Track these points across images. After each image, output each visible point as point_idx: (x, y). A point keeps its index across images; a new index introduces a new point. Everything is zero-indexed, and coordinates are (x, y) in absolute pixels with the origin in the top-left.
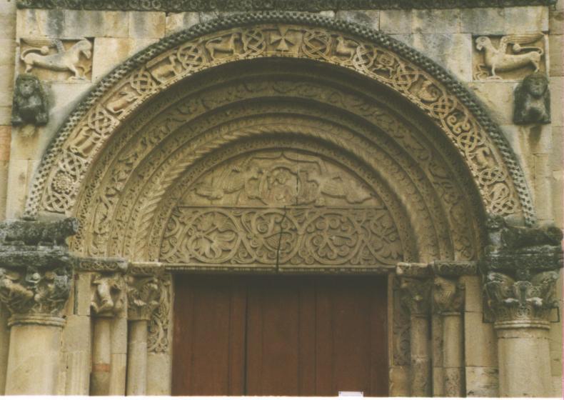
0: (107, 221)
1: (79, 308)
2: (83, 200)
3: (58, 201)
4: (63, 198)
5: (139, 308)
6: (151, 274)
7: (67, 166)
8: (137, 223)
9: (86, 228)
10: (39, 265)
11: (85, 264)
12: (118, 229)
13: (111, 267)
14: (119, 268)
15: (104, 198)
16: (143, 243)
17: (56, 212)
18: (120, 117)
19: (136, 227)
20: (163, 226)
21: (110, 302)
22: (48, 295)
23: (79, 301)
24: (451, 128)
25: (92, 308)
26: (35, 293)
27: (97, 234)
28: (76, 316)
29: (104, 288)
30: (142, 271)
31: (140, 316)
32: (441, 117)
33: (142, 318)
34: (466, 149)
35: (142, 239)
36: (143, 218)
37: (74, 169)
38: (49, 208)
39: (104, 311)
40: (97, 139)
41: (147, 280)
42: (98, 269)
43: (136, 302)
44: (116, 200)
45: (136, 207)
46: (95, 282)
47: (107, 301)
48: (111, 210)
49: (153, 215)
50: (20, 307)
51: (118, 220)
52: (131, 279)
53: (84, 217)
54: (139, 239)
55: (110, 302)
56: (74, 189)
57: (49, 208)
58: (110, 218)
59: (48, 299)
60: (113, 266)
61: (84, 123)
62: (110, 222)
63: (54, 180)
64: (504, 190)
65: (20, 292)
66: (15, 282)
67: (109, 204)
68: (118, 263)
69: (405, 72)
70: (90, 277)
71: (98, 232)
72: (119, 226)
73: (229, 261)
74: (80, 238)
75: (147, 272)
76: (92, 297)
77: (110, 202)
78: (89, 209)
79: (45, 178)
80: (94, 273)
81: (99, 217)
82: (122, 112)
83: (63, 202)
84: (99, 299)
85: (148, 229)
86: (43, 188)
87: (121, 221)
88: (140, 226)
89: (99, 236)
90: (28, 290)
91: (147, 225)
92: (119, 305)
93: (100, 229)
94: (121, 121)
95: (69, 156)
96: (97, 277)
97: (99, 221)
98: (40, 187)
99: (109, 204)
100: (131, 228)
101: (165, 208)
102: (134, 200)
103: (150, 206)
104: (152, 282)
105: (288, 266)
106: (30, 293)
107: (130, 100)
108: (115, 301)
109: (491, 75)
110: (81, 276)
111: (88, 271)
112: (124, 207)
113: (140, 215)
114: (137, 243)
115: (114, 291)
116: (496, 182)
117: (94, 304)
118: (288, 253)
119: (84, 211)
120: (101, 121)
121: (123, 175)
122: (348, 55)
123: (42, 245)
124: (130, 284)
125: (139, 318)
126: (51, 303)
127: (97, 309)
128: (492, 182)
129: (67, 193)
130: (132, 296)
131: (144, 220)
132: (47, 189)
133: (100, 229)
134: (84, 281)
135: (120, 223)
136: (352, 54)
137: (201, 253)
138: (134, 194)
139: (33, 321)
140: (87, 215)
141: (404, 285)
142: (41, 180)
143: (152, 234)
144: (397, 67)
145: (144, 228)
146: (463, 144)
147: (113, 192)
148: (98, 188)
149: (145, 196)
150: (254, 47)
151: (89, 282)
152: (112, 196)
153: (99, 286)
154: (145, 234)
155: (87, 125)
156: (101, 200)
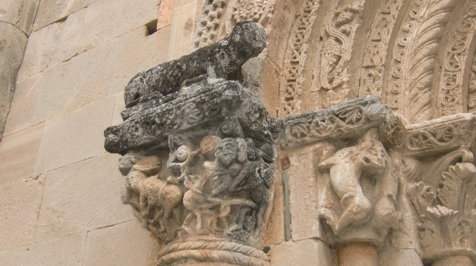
0: (341, 63)
1: (294, 226)
2: (293, 36)
5: (442, 220)
6: (452, 143)
8: (406, 65)
9: (301, 80)
10: (185, 126)
11: (295, 130)
12: (369, 81)
13: (351, 122)
14: (368, 120)
15: (332, 30)
16: (424, 98)
19: (404, 73)
20: (462, 66)
22: (206, 189)
23: (292, 211)
25: (322, 220)
26: (184, 190)
27: (327, 90)
28: (290, 242)
30: (431, 138)
31: (450, 244)
33: (456, 247)
35: (420, 89)
36: (415, 53)
39: (351, 225)
41: (449, 158)
42: (324, 134)
43: (429, 209)
44: (354, 26)
45: (400, 40)
46: (324, 163)
47: (352, 197)
48: (348, 43)
49: (435, 45)
50: (162, 228)
51: (368, 67)
52: (412, 165)
53: (298, 62)
54: (413, 92)
55: (360, 199)
56: (267, 10)
58: (346, 57)
59: (209, 199)
60: (355, 117)
62: (347, 63)
63: (235, 10)
65: (154, 192)
66: (148, 174)
67: (343, 37)
68: (363, 108)
70: (311, 156)
71: (327, 86)
72: (370, 75)
74: (292, 99)
75: (441, 140)
76: (323, 196)
77: (344, 32)
78: (305, 47)
79: (220, 10)
80: (318, 146)
81: (327, 61)
84: (338, 198)
85: (431, 70)
86: (217, 26)
87: (373, 67)
88: (413, 68)
89: (331, 91)
90: (169, 183)
91: (427, 63)
92: (385, 207)
93: (331, 81)
96: (325, 152)
97: (328, 69)
99: (343, 37)
100: (396, 78)
101: (459, 37)
102: (391, 27)
103: (425, 31)
104: (460, 160)
106: (174, 191)
108: (374, 201)
110: (293, 160)
111: (305, 144)
112: (374, 43)
113: (407, 52)
114: (414, 99)
115: (368, 176)
117: (328, 213)
119: (296, 53)
123: (188, 84)
124: (412, 178)
125: (447, 249)
126: (216, 208)
127: (336, 223)
130: (421, 201)
131: (419, 56)
132: (224, 27)
133: (331, 81)
134: (301, 165)
135: (372, 71)
138: (389, 17)
139: (184, 253)
140: (302, 59)
142: (214, 13)
143: (443, 85)
145: (421, 69)
147: (348, 15)
148: (317, 11)
149: (413, 19)
151: (311, 166)
152: (348, 21)
153: (332, 170)
154: (426, 79)
156: (328, 35)
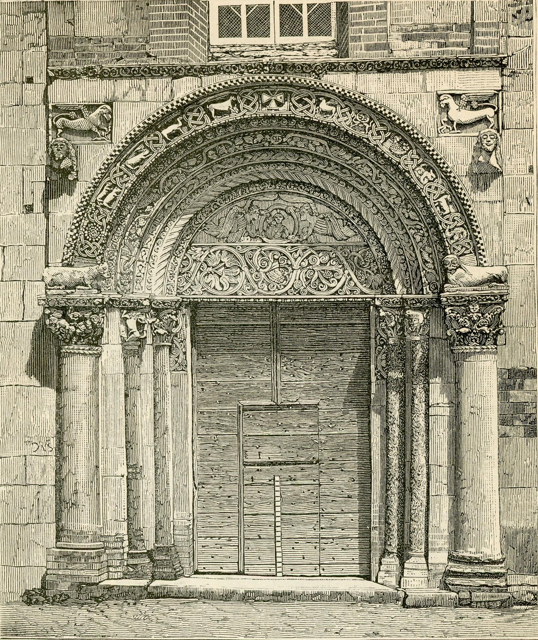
3: (89, 249)
4: (94, 245)
7: (95, 217)
17: (88, 257)
18: (137, 173)
21: (137, 334)
24: (419, 180)
29: (132, 324)
32: (410, 168)
34: (432, 197)
37: (101, 221)
38: (83, 255)
40: (118, 193)
55: (137, 334)
57: (83, 255)
61: (107, 180)
64: (462, 233)
69: (380, 128)
73: (236, 294)
82: (138, 169)
83: (94, 248)
84: (128, 331)
94: (138, 176)
95: (96, 208)
98: (74, 237)
105: (286, 296)
107: (144, 157)
109: (453, 129)
115: (140, 325)
116: (456, 227)
118: (285, 286)
120: (122, 177)
121: (141, 223)
122: (331, 113)
128: (451, 227)
129: (96, 241)
136: (333, 112)
137: (212, 287)
141: (382, 314)
144: (372, 124)
146: (429, 193)
150: (249, 107)
155: (110, 181)
